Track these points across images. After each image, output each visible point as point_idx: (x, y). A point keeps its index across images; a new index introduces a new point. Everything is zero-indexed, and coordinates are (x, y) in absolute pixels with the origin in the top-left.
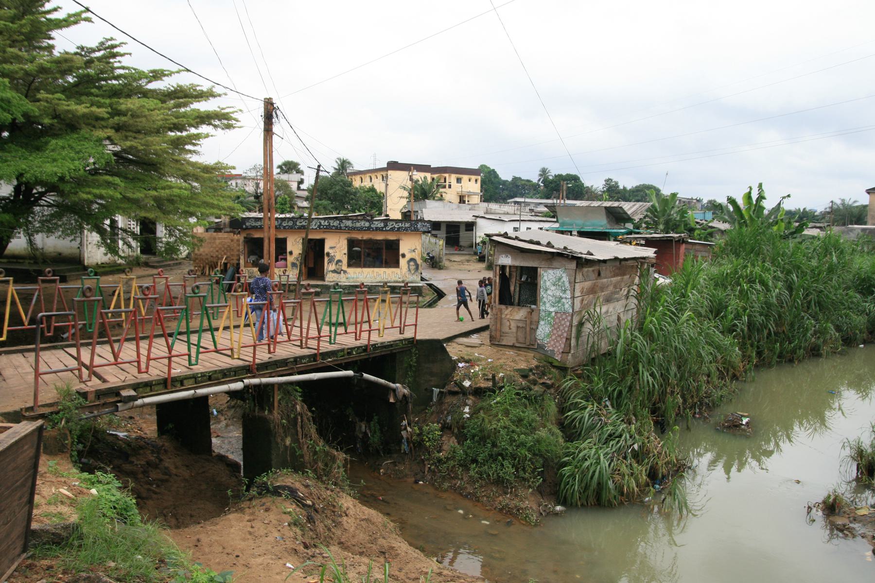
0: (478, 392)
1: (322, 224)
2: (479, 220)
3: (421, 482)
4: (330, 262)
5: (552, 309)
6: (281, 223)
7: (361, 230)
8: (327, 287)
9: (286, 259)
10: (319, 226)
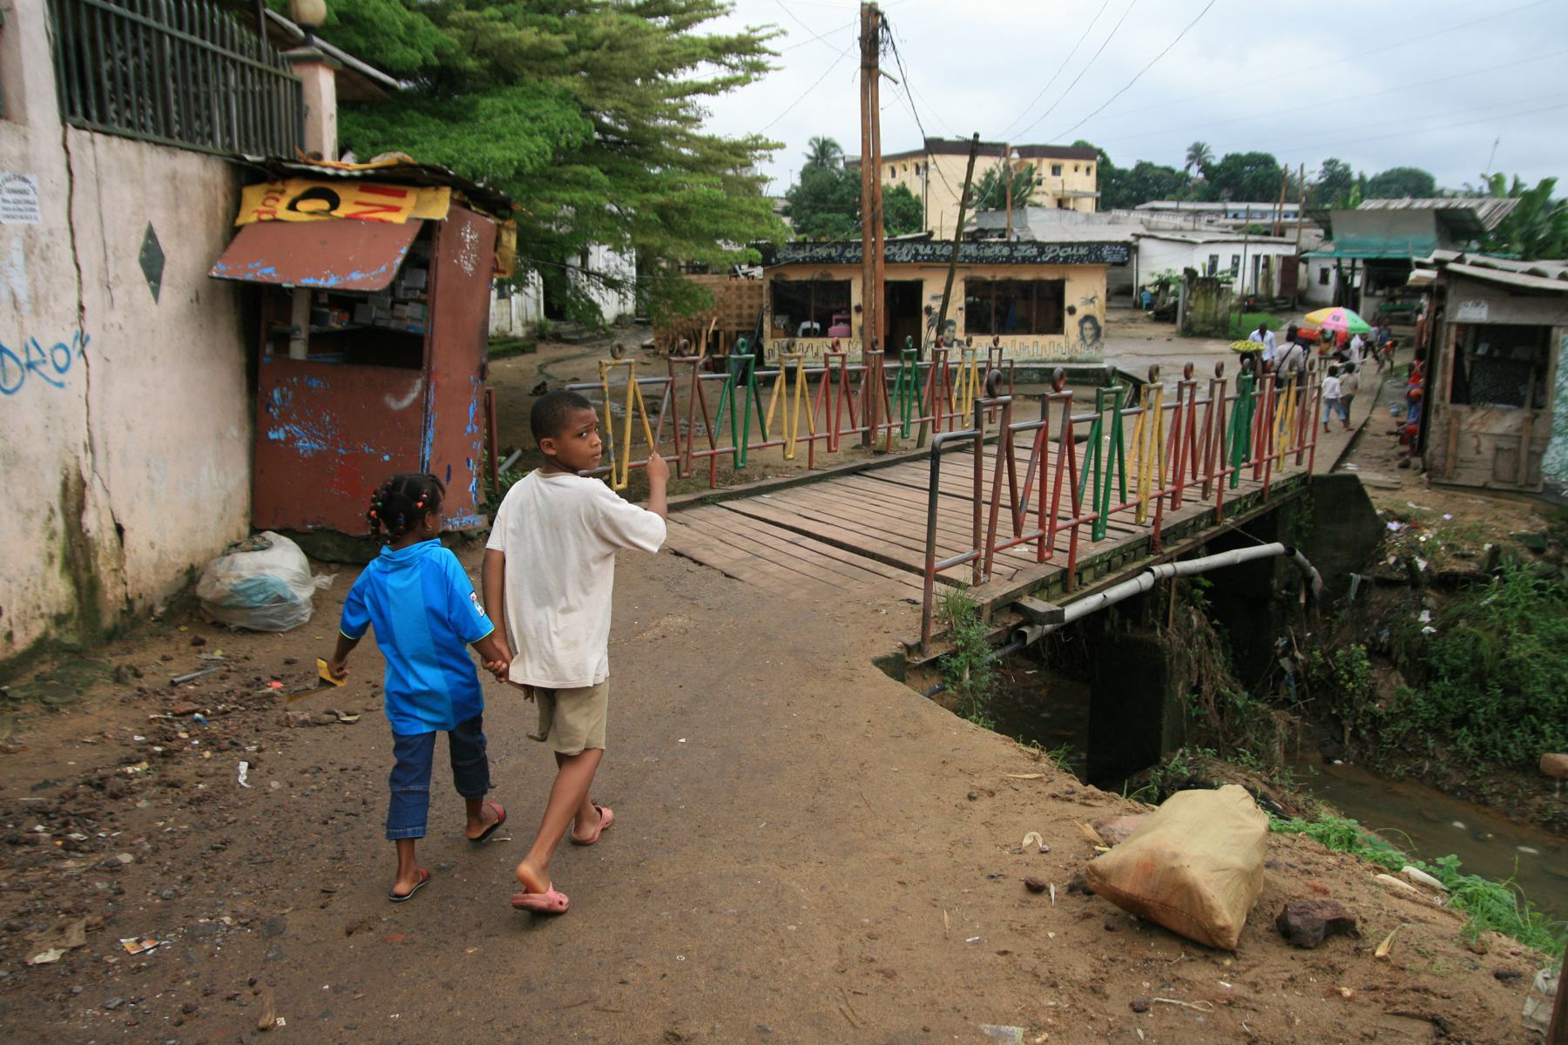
0: (1448, 583)
1: (921, 251)
2: (1143, 243)
3: (1338, 762)
6: (843, 252)
9: (848, 321)
10: (915, 257)
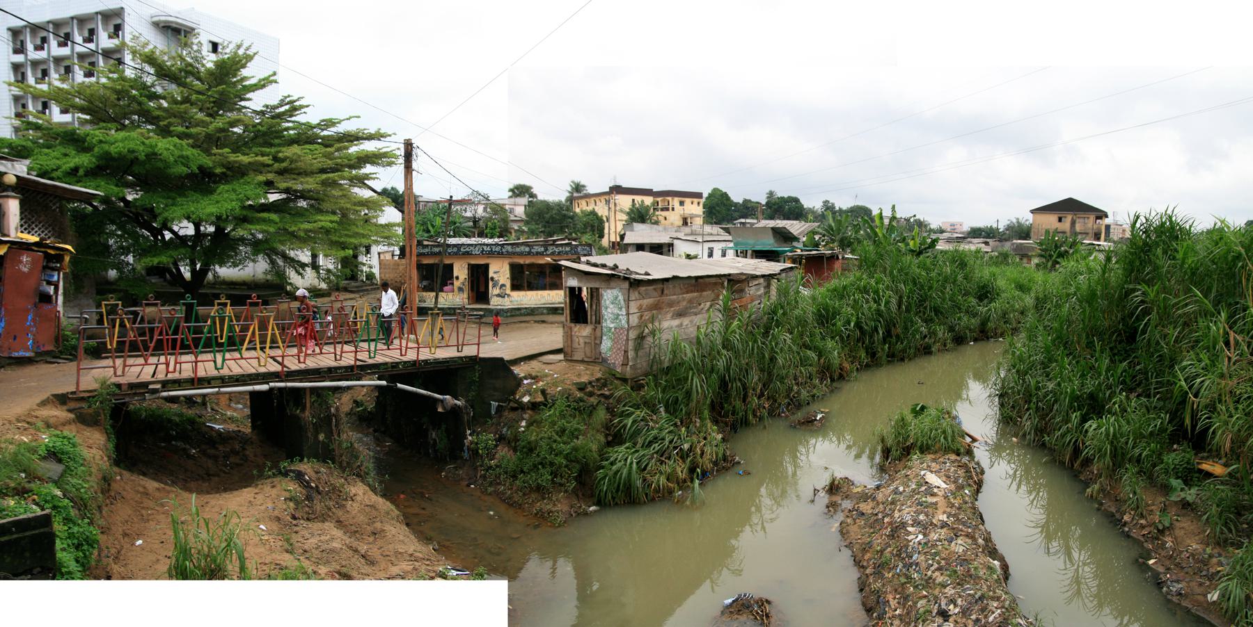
0: (534, 406)
4: (494, 286)
5: (612, 326)
7: (521, 254)
8: (490, 311)
9: (453, 284)
